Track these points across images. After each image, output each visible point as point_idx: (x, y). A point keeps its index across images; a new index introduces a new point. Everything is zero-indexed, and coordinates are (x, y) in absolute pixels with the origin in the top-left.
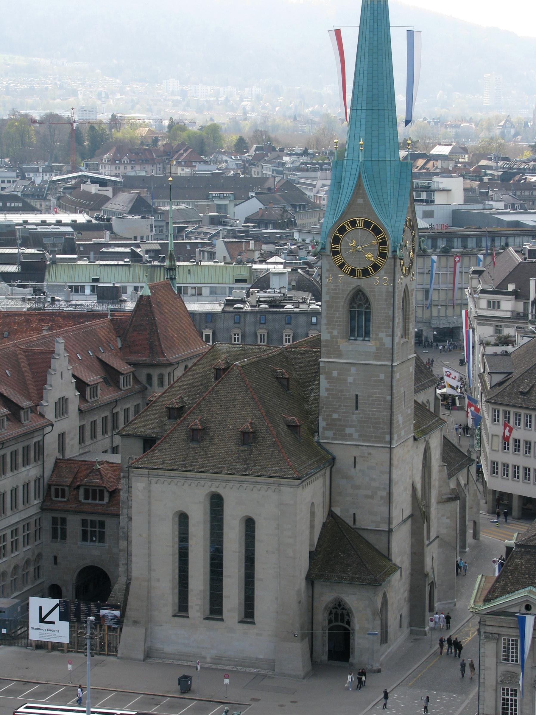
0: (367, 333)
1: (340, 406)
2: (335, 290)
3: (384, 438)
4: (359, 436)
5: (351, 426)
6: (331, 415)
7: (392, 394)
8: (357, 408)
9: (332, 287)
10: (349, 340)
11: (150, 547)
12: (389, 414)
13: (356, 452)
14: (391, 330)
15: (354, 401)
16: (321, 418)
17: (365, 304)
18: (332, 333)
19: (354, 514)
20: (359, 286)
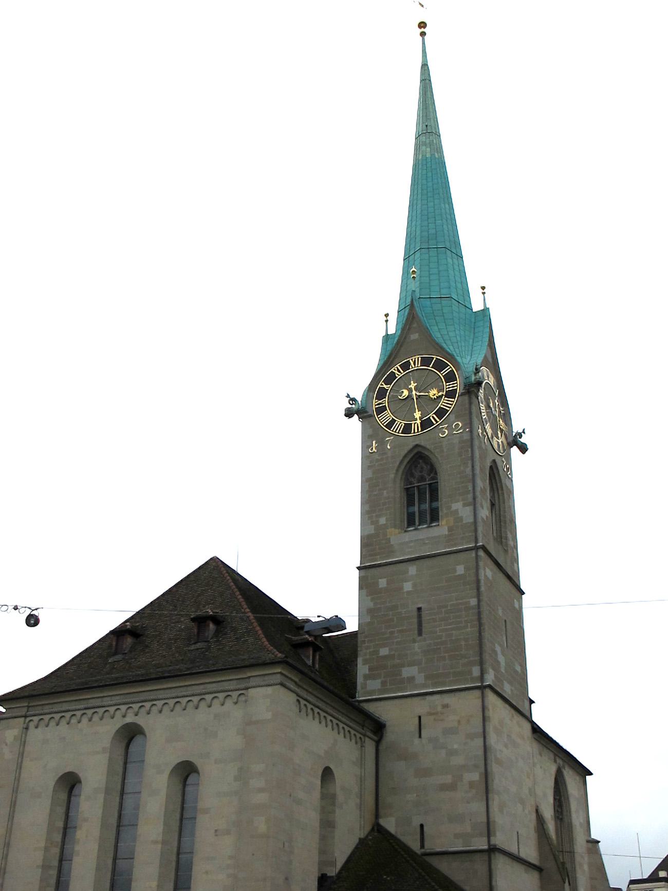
0: (434, 516)
1: (392, 633)
2: (382, 459)
3: (470, 672)
4: (427, 678)
5: (411, 664)
6: (377, 652)
7: (479, 595)
8: (420, 633)
9: (377, 457)
10: (406, 531)
11: (7, 855)
12: (476, 629)
13: (420, 707)
14: (470, 496)
15: (415, 620)
16: (360, 660)
17: (429, 475)
18: (378, 521)
19: (422, 826)
20: (417, 446)
